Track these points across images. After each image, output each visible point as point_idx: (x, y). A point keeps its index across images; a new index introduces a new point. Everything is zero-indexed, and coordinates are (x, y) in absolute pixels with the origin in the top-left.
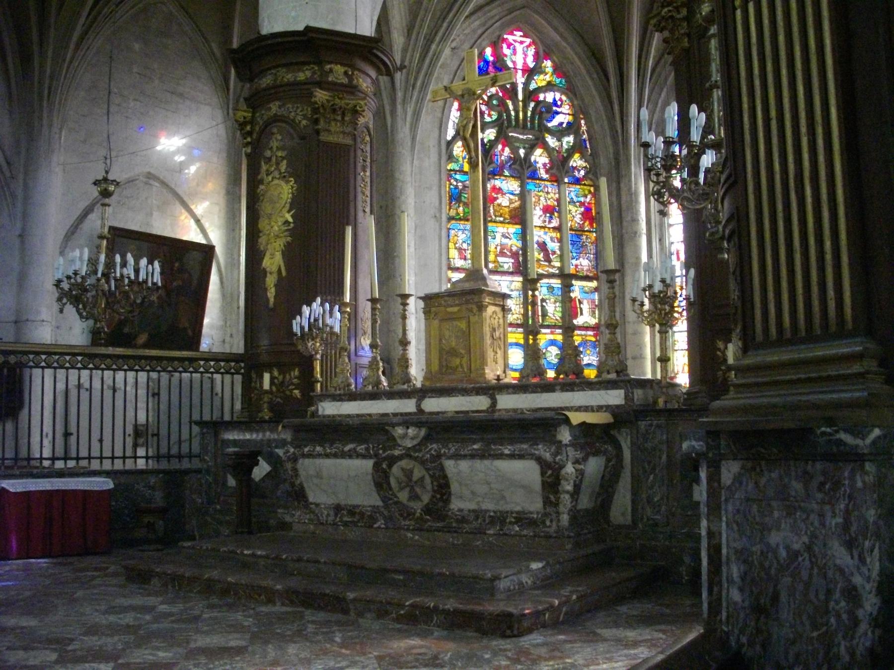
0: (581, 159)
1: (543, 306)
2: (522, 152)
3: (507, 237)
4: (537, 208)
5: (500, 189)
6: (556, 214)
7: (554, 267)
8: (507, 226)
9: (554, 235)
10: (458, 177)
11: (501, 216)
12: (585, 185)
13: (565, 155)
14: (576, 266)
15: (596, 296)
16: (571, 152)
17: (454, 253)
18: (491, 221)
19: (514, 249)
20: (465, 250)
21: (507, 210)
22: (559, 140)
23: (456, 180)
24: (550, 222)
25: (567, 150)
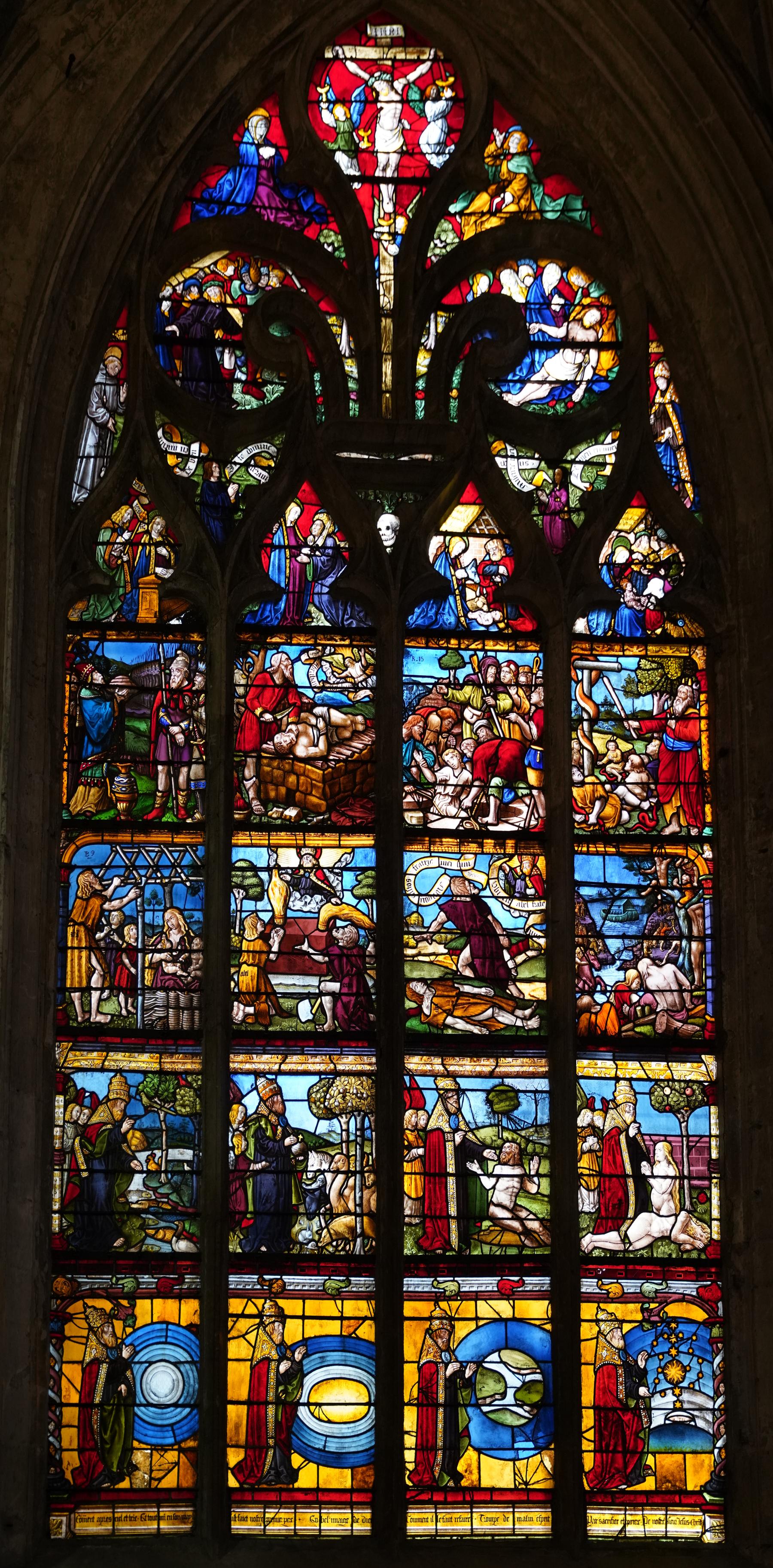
0: (650, 532)
1: (465, 1178)
2: (387, 522)
3: (314, 890)
4: (451, 757)
5: (289, 684)
6: (532, 776)
7: (521, 1003)
8: (314, 840)
9: (522, 864)
10: (113, 651)
11: (289, 801)
12: (666, 639)
13: (577, 519)
14: (621, 992)
15: (706, 1122)
16: (603, 508)
17: (80, 965)
18: (246, 826)
19: (343, 935)
20: (132, 951)
21: (316, 773)
22: (555, 459)
23: (105, 666)
24: (505, 812)
25: (587, 497)
